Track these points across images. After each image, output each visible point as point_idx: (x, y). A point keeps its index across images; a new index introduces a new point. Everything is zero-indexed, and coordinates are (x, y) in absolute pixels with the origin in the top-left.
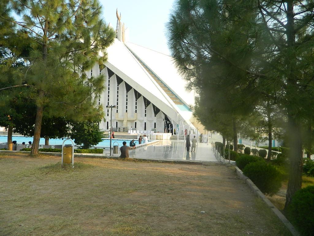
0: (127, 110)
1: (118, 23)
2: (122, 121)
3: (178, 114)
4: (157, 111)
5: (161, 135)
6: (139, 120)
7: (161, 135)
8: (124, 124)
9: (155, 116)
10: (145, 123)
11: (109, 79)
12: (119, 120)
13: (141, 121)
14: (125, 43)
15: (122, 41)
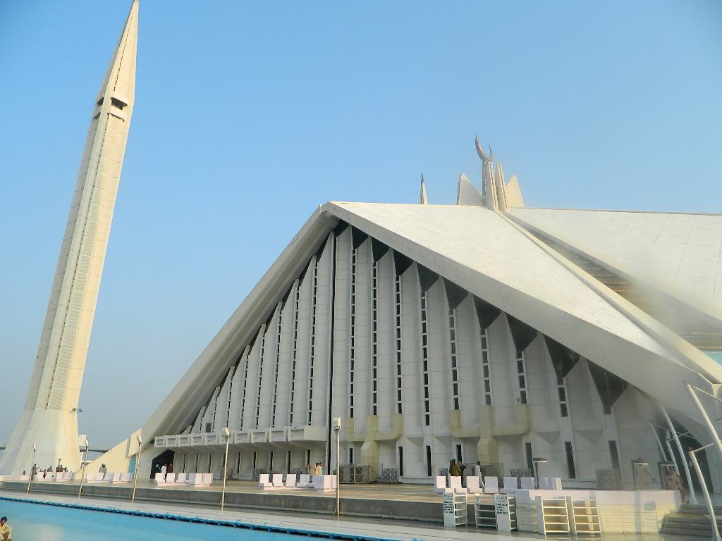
0: (488, 397)
1: (485, 177)
2: (473, 441)
3: (715, 387)
4: (612, 388)
5: (588, 502)
6: (541, 434)
7: (588, 502)
8: (479, 452)
9: (607, 411)
10: (568, 445)
11: (423, 295)
12: (465, 440)
13: (552, 438)
14: (508, 210)
15: (496, 209)
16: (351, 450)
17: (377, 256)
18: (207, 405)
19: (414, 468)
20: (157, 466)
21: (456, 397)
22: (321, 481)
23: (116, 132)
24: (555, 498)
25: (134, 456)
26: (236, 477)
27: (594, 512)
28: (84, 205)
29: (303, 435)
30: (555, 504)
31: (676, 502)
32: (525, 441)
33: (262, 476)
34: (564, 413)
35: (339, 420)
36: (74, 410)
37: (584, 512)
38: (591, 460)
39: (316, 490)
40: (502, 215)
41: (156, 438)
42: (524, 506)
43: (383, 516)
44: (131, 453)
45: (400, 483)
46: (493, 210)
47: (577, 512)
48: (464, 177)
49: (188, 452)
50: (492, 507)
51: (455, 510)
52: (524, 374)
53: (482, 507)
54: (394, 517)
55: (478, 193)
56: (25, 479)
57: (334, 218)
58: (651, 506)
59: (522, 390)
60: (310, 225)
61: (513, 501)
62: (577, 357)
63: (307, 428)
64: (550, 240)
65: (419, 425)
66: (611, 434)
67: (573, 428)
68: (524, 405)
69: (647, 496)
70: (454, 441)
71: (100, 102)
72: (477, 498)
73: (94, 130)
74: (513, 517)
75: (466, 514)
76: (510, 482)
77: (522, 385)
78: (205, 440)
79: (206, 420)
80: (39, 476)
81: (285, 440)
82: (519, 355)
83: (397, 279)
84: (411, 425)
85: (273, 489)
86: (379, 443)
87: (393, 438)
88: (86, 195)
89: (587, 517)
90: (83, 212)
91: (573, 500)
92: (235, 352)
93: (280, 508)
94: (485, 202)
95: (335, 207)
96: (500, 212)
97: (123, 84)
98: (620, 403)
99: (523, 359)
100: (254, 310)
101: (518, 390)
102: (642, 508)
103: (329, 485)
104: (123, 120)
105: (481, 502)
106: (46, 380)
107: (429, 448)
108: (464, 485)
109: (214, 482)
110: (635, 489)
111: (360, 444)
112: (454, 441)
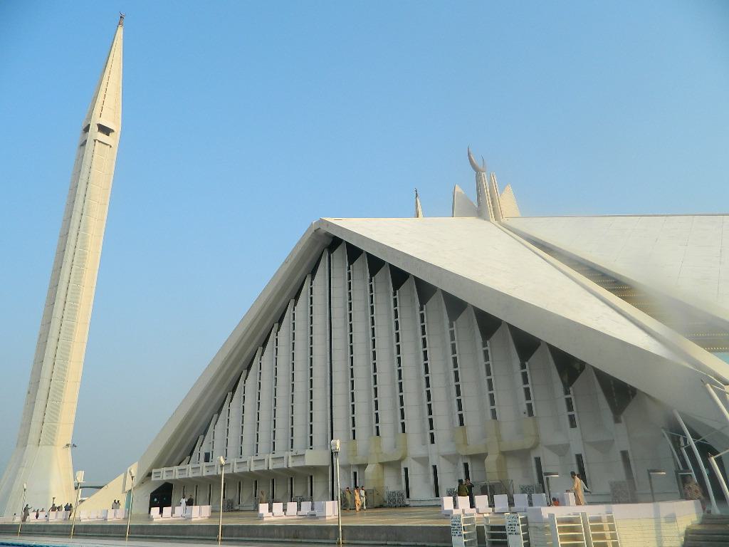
0: (494, 412)
2: (480, 458)
4: (620, 395)
5: (604, 517)
6: (553, 448)
7: (604, 517)
9: (617, 420)
11: (422, 309)
12: (472, 457)
13: (561, 450)
15: (493, 220)
16: (355, 473)
17: (373, 273)
18: (205, 434)
19: (421, 490)
20: (156, 500)
21: (460, 412)
22: (323, 509)
23: (103, 160)
24: (569, 514)
25: (130, 491)
26: (237, 508)
27: (612, 528)
28: (73, 233)
29: (304, 460)
30: (570, 521)
31: (697, 513)
32: (533, 455)
33: (261, 506)
34: (573, 424)
35: (338, 443)
36: (68, 445)
37: (601, 528)
38: (605, 472)
39: (318, 518)
40: (497, 224)
41: (154, 471)
42: (537, 525)
43: (388, 543)
44: (127, 489)
45: (407, 506)
46: (489, 221)
47: (594, 528)
48: (458, 189)
49: (186, 484)
50: (503, 528)
51: (464, 533)
52: (529, 386)
53: (493, 528)
54: (399, 543)
55: (472, 203)
56: (18, 520)
57: (327, 234)
58: (672, 519)
59: (529, 402)
60: (303, 243)
61: (525, 521)
62: (583, 365)
63: (308, 452)
64: (548, 248)
65: (424, 444)
66: (623, 443)
67: (583, 440)
68: (531, 418)
69: (667, 507)
70: (460, 460)
71: (87, 129)
72: (487, 518)
73: (80, 158)
74: (526, 537)
75: (476, 538)
76: (521, 499)
77: (528, 397)
78: (204, 471)
79: (204, 449)
80: (32, 516)
81: (285, 467)
82: (523, 367)
83: (395, 294)
84: (415, 444)
85: (273, 518)
86: (384, 465)
87: (398, 459)
88: (75, 224)
89: (604, 534)
90: (71, 240)
91: (588, 516)
92: (233, 375)
93: (280, 540)
94: (480, 212)
95: (329, 224)
96: (496, 222)
97: (109, 110)
98: (630, 411)
99: (527, 370)
100: (250, 332)
101: (524, 402)
102: (663, 520)
103: (331, 511)
104: (111, 147)
105: (490, 522)
106: (37, 415)
107: (435, 467)
108: (472, 506)
109: (214, 514)
110: (654, 501)
111: (363, 466)
112: (460, 460)
